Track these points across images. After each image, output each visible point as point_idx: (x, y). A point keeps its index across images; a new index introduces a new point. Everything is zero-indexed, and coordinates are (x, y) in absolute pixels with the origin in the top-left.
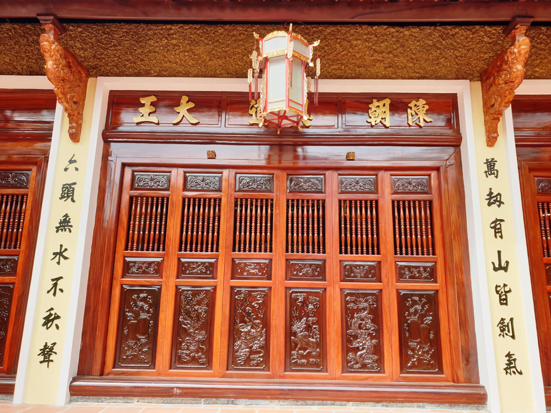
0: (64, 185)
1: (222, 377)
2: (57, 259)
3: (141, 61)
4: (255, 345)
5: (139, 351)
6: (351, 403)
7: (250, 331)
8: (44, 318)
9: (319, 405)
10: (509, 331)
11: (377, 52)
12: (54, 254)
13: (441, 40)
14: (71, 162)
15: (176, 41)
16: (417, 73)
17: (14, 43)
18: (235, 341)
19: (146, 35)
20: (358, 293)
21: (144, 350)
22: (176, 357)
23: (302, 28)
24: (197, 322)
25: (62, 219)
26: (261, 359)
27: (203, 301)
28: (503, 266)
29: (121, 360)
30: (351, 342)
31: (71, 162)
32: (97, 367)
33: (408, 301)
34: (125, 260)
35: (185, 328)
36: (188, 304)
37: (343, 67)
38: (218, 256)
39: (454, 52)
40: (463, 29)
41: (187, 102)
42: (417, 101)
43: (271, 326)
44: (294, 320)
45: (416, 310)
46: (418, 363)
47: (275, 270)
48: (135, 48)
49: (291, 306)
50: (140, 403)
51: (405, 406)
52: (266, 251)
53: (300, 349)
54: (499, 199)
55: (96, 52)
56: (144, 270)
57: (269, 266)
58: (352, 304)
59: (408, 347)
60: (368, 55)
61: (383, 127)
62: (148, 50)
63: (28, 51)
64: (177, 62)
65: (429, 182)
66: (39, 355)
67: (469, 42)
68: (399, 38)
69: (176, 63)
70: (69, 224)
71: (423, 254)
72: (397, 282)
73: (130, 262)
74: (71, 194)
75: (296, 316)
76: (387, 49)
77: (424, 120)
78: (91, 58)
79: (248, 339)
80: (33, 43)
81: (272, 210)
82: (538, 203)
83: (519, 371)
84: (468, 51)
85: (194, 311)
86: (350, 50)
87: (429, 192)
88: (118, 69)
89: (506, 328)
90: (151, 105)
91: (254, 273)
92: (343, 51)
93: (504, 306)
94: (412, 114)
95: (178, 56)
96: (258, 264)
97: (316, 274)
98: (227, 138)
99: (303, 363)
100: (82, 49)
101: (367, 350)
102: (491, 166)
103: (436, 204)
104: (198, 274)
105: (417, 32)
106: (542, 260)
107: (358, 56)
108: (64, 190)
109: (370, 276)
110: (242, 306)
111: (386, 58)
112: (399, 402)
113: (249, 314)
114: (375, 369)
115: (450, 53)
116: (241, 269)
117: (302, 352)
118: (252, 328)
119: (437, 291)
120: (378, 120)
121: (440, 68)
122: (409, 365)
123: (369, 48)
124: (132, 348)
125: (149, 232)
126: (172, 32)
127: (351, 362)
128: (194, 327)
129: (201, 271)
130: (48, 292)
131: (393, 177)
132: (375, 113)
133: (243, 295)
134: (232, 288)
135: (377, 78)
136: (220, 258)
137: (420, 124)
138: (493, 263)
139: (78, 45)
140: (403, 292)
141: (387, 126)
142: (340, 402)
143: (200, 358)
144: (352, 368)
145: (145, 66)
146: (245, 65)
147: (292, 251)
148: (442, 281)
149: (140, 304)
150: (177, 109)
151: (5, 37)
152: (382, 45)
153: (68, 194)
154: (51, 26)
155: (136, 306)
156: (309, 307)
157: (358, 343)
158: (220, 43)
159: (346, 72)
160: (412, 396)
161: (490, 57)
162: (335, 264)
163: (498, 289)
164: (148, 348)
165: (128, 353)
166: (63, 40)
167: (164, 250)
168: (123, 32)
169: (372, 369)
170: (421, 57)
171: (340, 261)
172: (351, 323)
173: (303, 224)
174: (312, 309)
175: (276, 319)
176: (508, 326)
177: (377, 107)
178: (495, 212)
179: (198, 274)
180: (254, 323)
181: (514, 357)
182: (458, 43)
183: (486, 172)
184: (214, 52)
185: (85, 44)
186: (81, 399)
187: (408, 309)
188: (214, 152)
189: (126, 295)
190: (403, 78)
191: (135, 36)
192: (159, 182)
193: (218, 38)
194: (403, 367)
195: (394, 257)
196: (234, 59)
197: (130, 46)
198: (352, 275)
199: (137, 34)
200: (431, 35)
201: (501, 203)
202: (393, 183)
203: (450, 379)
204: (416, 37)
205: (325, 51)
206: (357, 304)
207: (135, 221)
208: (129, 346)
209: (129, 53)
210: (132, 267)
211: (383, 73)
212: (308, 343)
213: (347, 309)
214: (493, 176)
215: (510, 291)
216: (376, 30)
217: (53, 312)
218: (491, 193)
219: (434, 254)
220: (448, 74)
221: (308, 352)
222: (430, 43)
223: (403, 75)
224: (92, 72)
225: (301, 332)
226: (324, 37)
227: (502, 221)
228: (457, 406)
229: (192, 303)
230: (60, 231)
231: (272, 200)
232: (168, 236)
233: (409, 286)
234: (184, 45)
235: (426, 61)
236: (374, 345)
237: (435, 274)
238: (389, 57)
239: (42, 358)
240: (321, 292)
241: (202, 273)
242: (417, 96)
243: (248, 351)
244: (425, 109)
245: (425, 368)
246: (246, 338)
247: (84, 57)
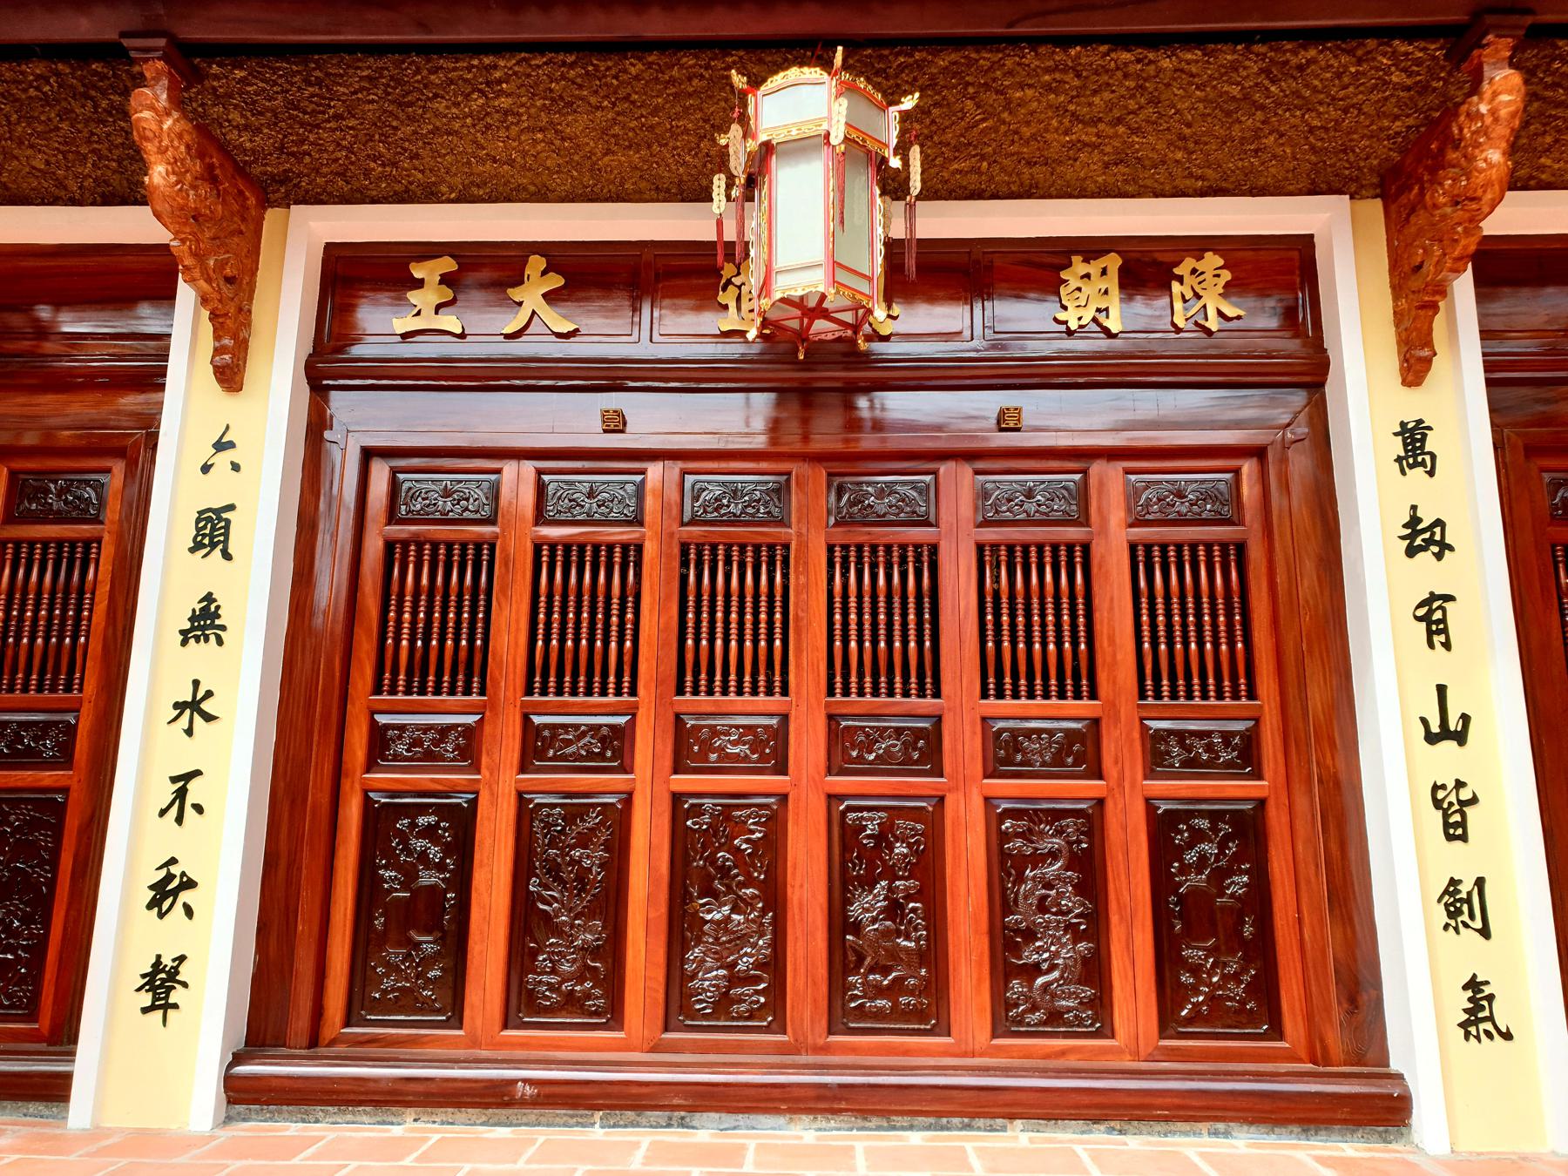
1: (653, 1050)
2: (184, 721)
3: (411, 158)
4: (745, 959)
5: (417, 979)
6: (1018, 1123)
7: (728, 919)
8: (151, 887)
9: (929, 1128)
10: (1472, 916)
11: (1081, 122)
12: (176, 705)
13: (1266, 82)
14: (220, 446)
15: (510, 100)
16: (1197, 179)
17: (58, 115)
18: (685, 948)
19: (426, 86)
20: (1035, 811)
21: (431, 974)
22: (520, 993)
23: (866, 56)
24: (579, 895)
25: (198, 607)
26: (762, 1000)
27: (596, 836)
28: (1452, 728)
29: (366, 1003)
30: (1016, 950)
31: (220, 446)
32: (300, 1023)
33: (1181, 832)
34: (373, 723)
35: (545, 911)
36: (551, 845)
37: (985, 164)
38: (636, 706)
39: (1303, 115)
40: (1329, 49)
41: (544, 273)
43: (789, 905)
44: (854, 886)
45: (1203, 858)
46: (1210, 1010)
47: (799, 745)
48: (395, 124)
49: (845, 848)
50: (423, 1125)
51: (1174, 1133)
52: (769, 692)
53: (872, 970)
54: (1437, 538)
55: (285, 136)
57: (780, 735)
58: (1019, 843)
59: (1183, 963)
60: (1057, 130)
61: (1102, 335)
62: (430, 127)
63: (96, 138)
64: (514, 160)
65: (1234, 491)
66: (139, 990)
67: (1345, 87)
68: (1146, 80)
69: (511, 162)
70: (217, 622)
71: (1220, 696)
72: (1146, 778)
73: (387, 727)
74: (222, 538)
75: (859, 876)
76: (1111, 110)
77: (1220, 314)
78: (271, 154)
79: (725, 942)
80: (111, 115)
81: (785, 576)
83: (1504, 1030)
84: (1345, 111)
85: (569, 864)
86: (1005, 115)
87: (1235, 519)
88: (348, 183)
89: (1465, 908)
90: (441, 283)
91: (738, 755)
92: (983, 120)
93: (1458, 844)
94: (1183, 296)
96: (750, 729)
97: (916, 755)
98: (658, 374)
99: (881, 1009)
100: (246, 127)
101: (1063, 972)
102: (1414, 441)
103: (1256, 553)
104: (580, 758)
105: (1197, 62)
107: (1026, 132)
108: (201, 525)
109: (1070, 760)
110: (704, 848)
111: (1107, 137)
112: (1158, 1119)
113: (724, 872)
114: (1086, 1027)
115: (1292, 120)
116: (702, 743)
117: (878, 977)
118: (733, 910)
119: (1261, 803)
120: (1088, 315)
121: (1263, 164)
122: (1183, 1013)
123: (1060, 110)
124: (397, 969)
125: (442, 641)
126: (498, 74)
127: (1017, 1005)
128: (570, 910)
129: (587, 751)
130: (163, 813)
131: (1133, 477)
132: (1077, 294)
133: (706, 818)
134: (677, 798)
135: (1083, 194)
137: (1207, 325)
138: (1424, 721)
139: (235, 116)
140: (1163, 807)
141: (1114, 331)
142: (989, 1122)
143: (588, 996)
144: (1020, 1023)
145: (422, 172)
146: (705, 166)
147: (846, 692)
148: (1276, 772)
149: (419, 844)
150: (515, 294)
151: (31, 97)
152: (1097, 100)
153: (212, 537)
154: (160, 65)
155: (408, 851)
156: (897, 851)
157: (1038, 950)
158: (633, 103)
160: (1194, 1103)
161: (1409, 128)
162: (967, 728)
163: (1441, 794)
164: (442, 969)
165: (387, 983)
166: (194, 105)
167: (482, 692)
168: (362, 78)
169: (1078, 1026)
170: (1209, 133)
171: (984, 719)
172: (1017, 894)
173: (874, 614)
174: (905, 856)
175: (802, 886)
176: (1469, 901)
177: (1082, 277)
178: (1427, 573)
179: (580, 758)
180: (739, 897)
181: (1487, 990)
182: (1315, 90)
183: (1399, 460)
184: (616, 130)
185: (253, 115)
186: (257, 1113)
187: (1178, 853)
188: (619, 414)
189: (378, 820)
190: (1156, 195)
191: (395, 88)
192: (467, 500)
193: (629, 90)
194: (1167, 1021)
195: (1139, 706)
196: (675, 148)
197: (379, 117)
198: (1019, 757)
199: (399, 82)
200: (1236, 70)
201: (1445, 547)
202: (1133, 494)
203: (1303, 1054)
204: (1193, 76)
205: (933, 122)
206: (1032, 842)
207: (400, 612)
208: (387, 965)
209: (377, 137)
210: (394, 742)
211: (1100, 179)
212: (895, 954)
213: (1004, 855)
214: (1421, 469)
215: (1474, 800)
216: (1078, 56)
217: (175, 870)
218: (1414, 521)
219: (1252, 695)
220: (1287, 179)
221: (895, 979)
222: (1235, 91)
223: (1156, 185)
224: (274, 192)
225: (874, 920)
226: (930, 79)
227: (1449, 598)
228: (1323, 1133)
229: (563, 842)
230: (192, 641)
231: (786, 547)
232: (494, 654)
233: (1180, 788)
234: (533, 111)
235: (1225, 143)
236: (1084, 958)
237: (1255, 752)
238: (1116, 135)
239: (146, 999)
240: (930, 809)
241: (591, 756)
242: (1198, 245)
243: (724, 976)
244: (1222, 282)
245: (1230, 1022)
246: (717, 939)
247: (253, 151)
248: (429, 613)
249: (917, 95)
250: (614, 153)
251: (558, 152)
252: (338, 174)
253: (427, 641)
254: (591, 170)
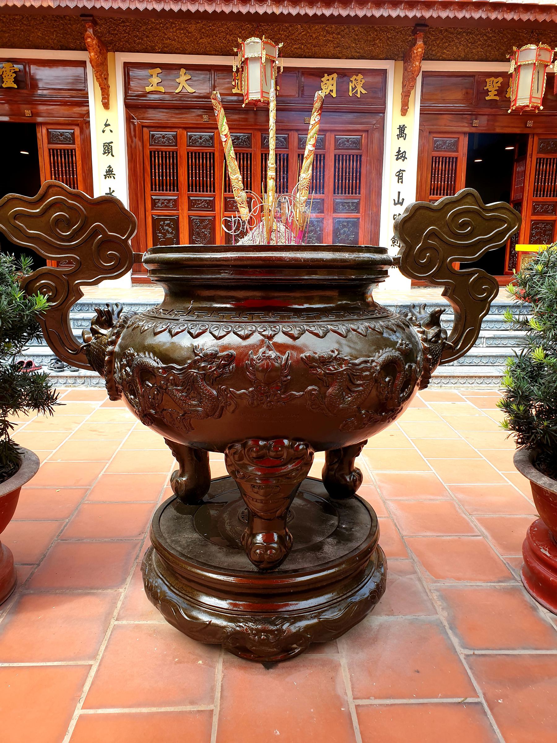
0: (104, 144)
10: (397, 243)
11: (329, 33)
14: (107, 125)
31: (107, 125)
34: (152, 198)
38: (215, 195)
42: (357, 75)
45: (344, 231)
48: (140, 25)
54: (404, 156)
55: (109, 28)
56: (166, 205)
60: (322, 35)
63: (55, 26)
70: (113, 173)
82: (433, 157)
84: (398, 33)
86: (309, 30)
88: (129, 44)
89: (396, 241)
92: (303, 32)
95: (175, 34)
102: (402, 130)
106: (428, 197)
107: (314, 36)
108: (105, 147)
111: (335, 38)
116: (230, 204)
125: (166, 177)
136: (216, 197)
138: (394, 200)
145: (150, 42)
149: (166, 228)
153: (108, 151)
154: (90, 24)
159: (305, 50)
161: (413, 39)
167: (177, 191)
178: (400, 165)
183: (398, 135)
184: (203, 30)
189: (155, 222)
196: (220, 37)
202: (336, 140)
205: (289, 32)
207: (155, 170)
211: (333, 52)
214: (402, 138)
218: (399, 151)
230: (107, 178)
231: (251, 154)
234: (179, 22)
238: (338, 38)
242: (357, 71)
244: (362, 83)
247: (101, 33)
248: (162, 170)
249: (283, 43)
250: (203, 38)
251: (187, 37)
252: (126, 42)
253: (163, 177)
254: (197, 43)
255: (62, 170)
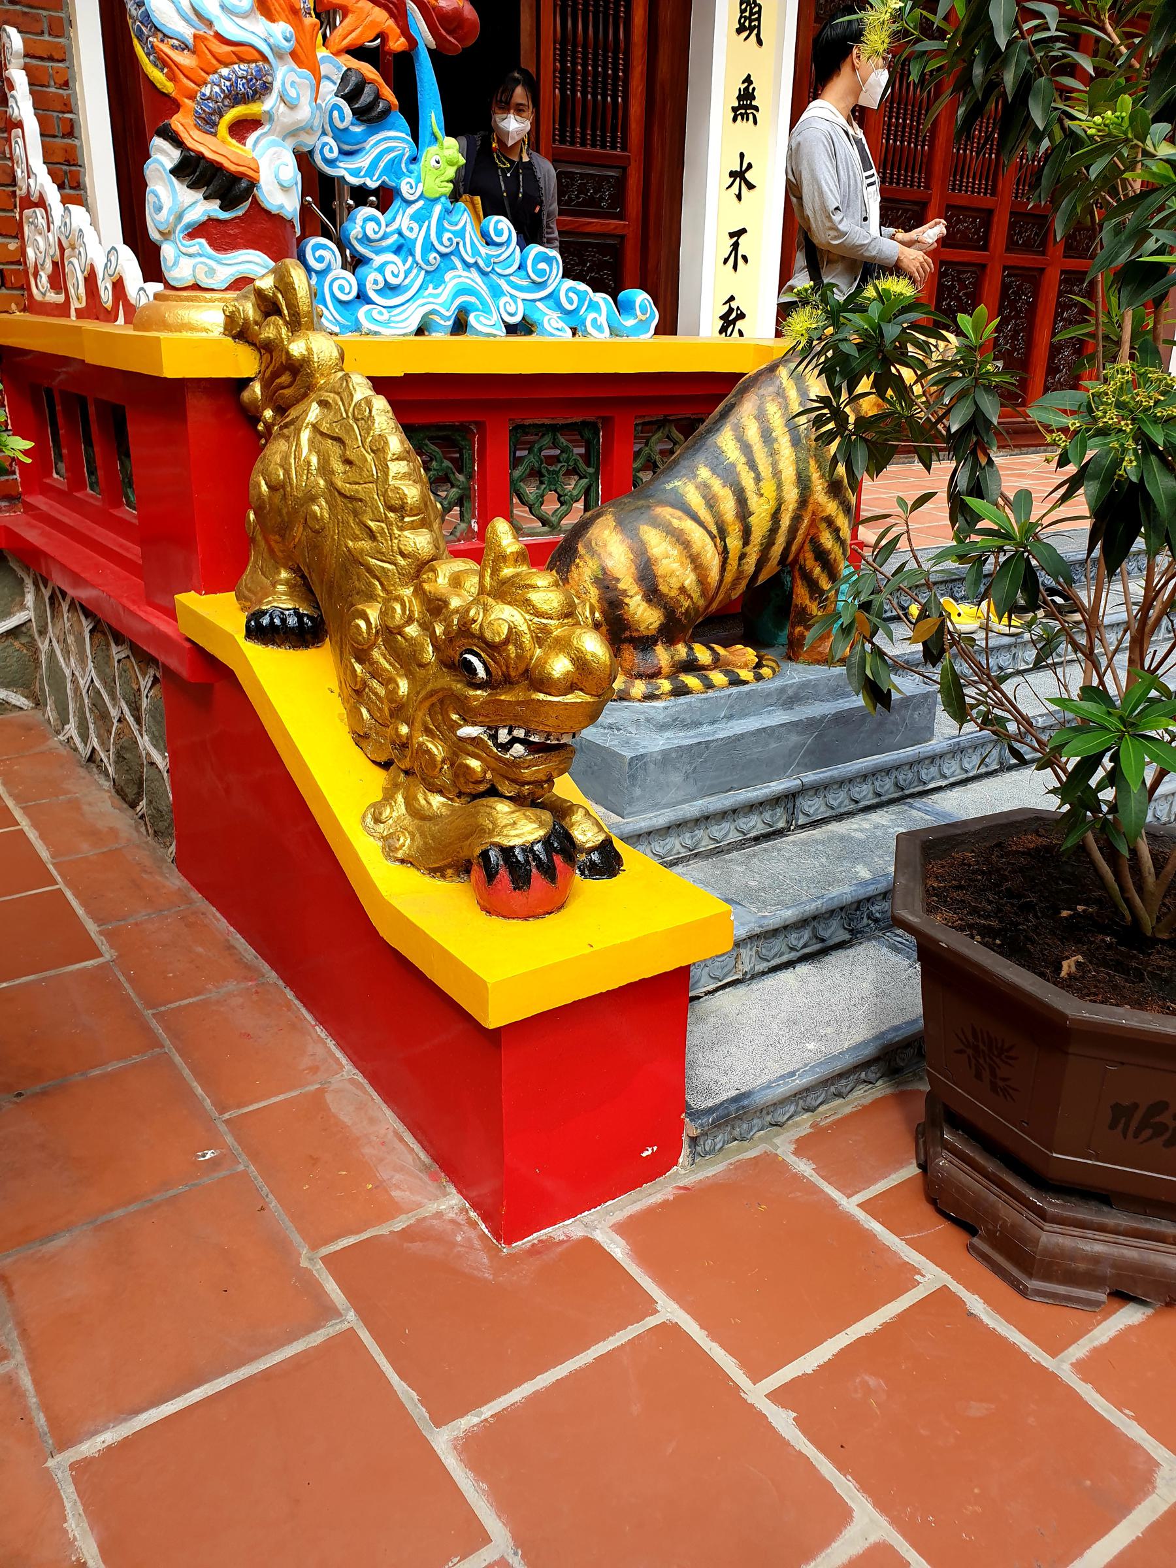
8: (721, 318)
108: (743, 7)
130: (726, 261)
230: (739, 117)
255: (585, 73)
